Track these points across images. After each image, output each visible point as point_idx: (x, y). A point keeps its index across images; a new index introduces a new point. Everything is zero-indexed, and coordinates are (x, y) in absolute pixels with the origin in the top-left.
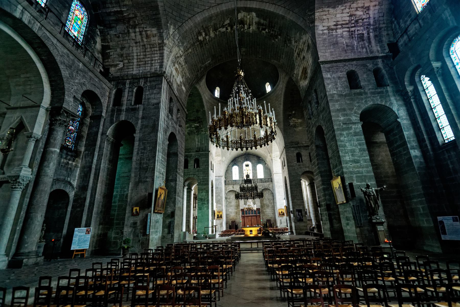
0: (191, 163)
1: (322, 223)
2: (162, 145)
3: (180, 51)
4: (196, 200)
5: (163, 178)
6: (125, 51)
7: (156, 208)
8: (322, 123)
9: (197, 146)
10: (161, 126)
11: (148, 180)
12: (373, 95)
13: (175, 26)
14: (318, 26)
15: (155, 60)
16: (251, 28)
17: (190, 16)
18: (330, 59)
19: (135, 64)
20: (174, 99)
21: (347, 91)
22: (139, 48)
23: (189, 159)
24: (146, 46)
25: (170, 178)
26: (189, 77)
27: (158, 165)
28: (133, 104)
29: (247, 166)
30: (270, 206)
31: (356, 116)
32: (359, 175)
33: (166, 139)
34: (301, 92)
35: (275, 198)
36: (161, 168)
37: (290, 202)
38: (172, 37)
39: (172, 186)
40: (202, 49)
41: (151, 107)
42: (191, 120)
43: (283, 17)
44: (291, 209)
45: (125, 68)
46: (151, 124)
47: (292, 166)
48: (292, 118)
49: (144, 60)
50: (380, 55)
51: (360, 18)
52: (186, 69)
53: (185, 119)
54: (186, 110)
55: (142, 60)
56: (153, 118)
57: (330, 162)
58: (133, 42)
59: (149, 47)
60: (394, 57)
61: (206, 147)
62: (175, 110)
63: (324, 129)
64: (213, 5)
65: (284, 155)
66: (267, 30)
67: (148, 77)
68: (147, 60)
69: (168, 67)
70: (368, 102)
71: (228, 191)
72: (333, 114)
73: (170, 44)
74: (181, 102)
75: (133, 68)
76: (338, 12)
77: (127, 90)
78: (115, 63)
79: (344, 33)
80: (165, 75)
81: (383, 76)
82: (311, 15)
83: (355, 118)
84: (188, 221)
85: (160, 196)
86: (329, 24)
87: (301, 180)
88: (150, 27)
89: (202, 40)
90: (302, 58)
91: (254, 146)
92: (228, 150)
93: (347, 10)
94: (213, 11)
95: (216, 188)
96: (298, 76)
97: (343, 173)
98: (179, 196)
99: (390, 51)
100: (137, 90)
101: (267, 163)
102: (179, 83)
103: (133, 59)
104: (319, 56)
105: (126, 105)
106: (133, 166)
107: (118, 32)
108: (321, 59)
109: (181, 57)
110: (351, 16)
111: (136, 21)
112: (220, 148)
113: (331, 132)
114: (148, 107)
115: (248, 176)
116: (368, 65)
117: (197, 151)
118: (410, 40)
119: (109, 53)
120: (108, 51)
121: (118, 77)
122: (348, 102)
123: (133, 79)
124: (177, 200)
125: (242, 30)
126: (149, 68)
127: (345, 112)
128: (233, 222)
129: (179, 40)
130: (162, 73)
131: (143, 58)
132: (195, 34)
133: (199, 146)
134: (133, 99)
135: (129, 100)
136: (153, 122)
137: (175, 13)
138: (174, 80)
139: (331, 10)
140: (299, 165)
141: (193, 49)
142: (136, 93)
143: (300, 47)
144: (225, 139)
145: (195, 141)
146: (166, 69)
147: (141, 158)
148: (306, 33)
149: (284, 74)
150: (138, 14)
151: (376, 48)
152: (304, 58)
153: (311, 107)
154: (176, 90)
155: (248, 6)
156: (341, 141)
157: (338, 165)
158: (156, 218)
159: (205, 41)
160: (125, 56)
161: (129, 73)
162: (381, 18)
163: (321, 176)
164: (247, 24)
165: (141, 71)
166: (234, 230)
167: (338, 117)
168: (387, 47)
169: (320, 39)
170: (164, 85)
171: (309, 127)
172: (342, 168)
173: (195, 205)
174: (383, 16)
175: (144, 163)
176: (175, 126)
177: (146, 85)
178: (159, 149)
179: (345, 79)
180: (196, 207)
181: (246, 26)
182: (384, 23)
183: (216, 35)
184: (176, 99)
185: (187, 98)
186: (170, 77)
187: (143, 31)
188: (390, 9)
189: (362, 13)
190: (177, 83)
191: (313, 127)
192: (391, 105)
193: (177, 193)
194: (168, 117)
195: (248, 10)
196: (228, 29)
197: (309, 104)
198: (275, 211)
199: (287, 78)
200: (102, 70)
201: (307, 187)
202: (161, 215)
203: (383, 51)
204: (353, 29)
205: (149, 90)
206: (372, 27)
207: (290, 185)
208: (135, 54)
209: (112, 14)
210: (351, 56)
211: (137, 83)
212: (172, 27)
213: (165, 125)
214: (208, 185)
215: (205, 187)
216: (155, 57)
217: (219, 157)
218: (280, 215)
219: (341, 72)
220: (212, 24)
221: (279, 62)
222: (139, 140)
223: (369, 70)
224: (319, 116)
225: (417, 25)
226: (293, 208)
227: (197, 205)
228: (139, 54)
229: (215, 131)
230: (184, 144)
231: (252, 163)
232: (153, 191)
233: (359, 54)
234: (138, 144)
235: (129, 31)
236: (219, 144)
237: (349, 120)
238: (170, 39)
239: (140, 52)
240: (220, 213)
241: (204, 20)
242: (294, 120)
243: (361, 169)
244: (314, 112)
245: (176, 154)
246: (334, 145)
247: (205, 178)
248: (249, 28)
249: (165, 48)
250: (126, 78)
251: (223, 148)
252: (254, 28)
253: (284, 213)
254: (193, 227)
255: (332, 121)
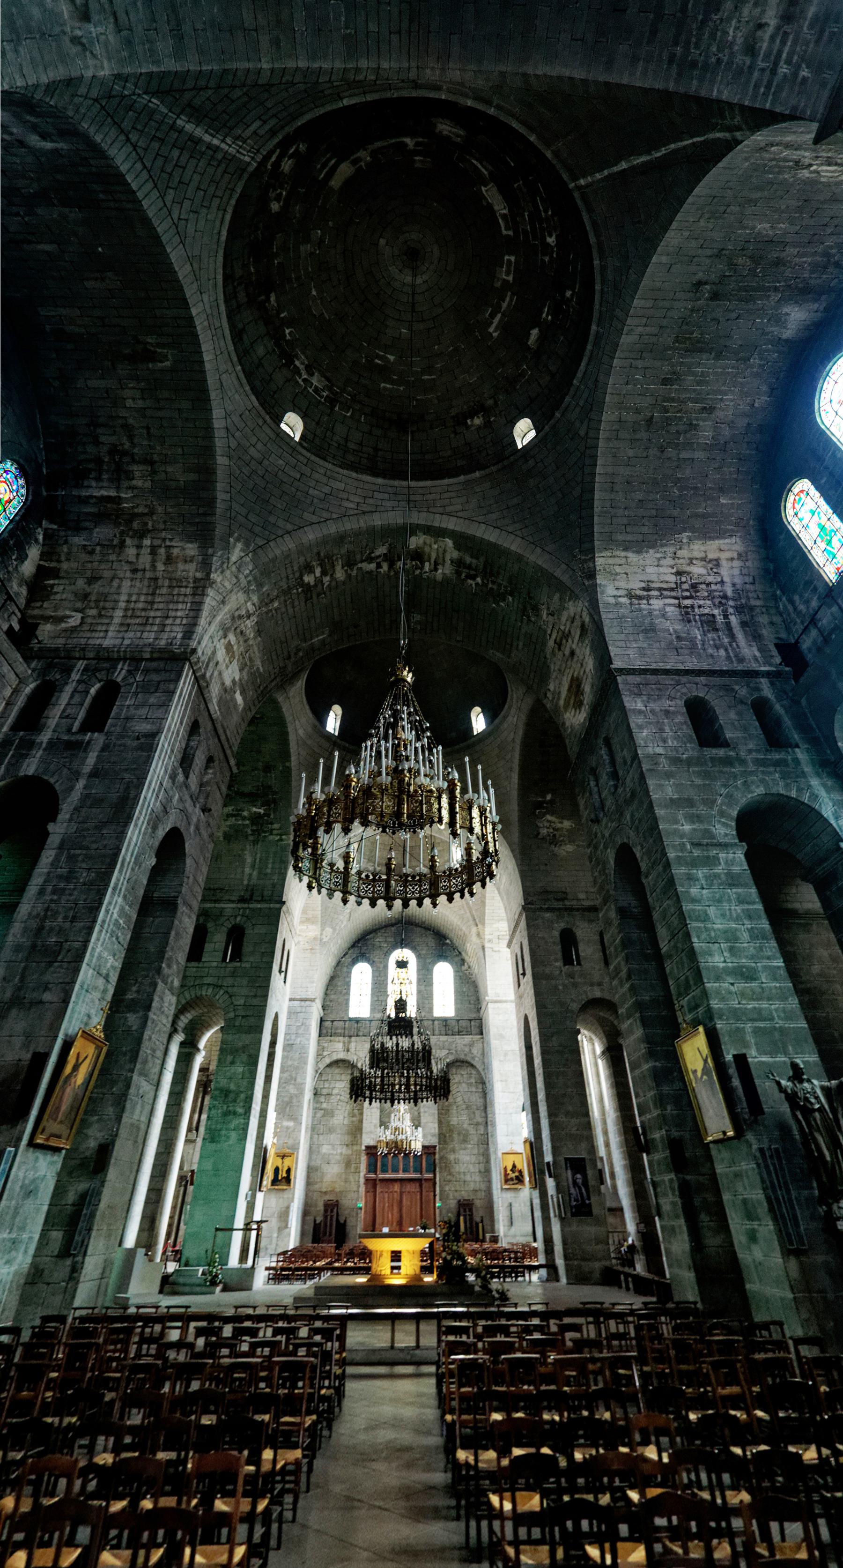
0: (217, 940)
1: (662, 1227)
2: (133, 869)
3: (249, 604)
4: (205, 1093)
5: (105, 991)
6: (96, 587)
7: (44, 1123)
8: (632, 837)
9: (245, 882)
10: (143, 805)
11: (47, 997)
12: (761, 769)
13: (247, 544)
14: (605, 586)
15: (176, 617)
16: (440, 571)
17: (289, 527)
18: (639, 664)
19: (116, 620)
20: (206, 726)
21: (691, 750)
22: (138, 584)
23: (210, 925)
24: (160, 582)
25: (129, 996)
26: (261, 670)
27: (98, 939)
28: (74, 729)
29: (402, 964)
30: (474, 1138)
31: (725, 825)
32: (761, 1024)
33: (151, 848)
34: (567, 741)
35: (492, 1105)
36: (105, 954)
37: (545, 1123)
38: (234, 568)
39: (129, 1031)
40: (309, 605)
41: (129, 742)
42: (242, 795)
43: (520, 558)
44: (548, 1158)
45: (86, 627)
46: (114, 796)
47: (548, 977)
48: (544, 814)
49: (143, 614)
50: (763, 669)
51: (702, 580)
52: (256, 649)
53: (224, 788)
54: (232, 762)
55: (138, 614)
56: (127, 776)
57: (668, 970)
58: (126, 567)
59: (167, 583)
60: (797, 676)
61: (274, 885)
62: (199, 760)
63: (638, 855)
64: (352, 512)
65: (522, 935)
66: (479, 580)
67: (142, 659)
68: (152, 614)
69: (206, 638)
70: (753, 787)
71: (328, 1061)
72: (659, 812)
73: (227, 584)
74: (223, 738)
75: (106, 631)
76: (648, 562)
77: (69, 689)
78: (60, 613)
79: (668, 609)
80: (194, 659)
81: (778, 722)
82: (585, 561)
83: (724, 830)
84: (153, 1197)
85: (76, 1068)
86: (630, 586)
87: (578, 1032)
88: (181, 540)
89: (312, 583)
90: (567, 652)
91: (430, 896)
92: (345, 901)
93: (669, 561)
94: (349, 525)
95: (288, 1047)
96: (559, 698)
97: (710, 1014)
98: (144, 1074)
99: (786, 661)
100: (98, 692)
101: (466, 958)
102: (228, 683)
103: (113, 609)
104: (612, 655)
105: (54, 731)
106: (10, 938)
107: (95, 540)
108: (617, 664)
109: (249, 617)
110: (679, 573)
111: (150, 524)
112: (319, 892)
113: (660, 868)
114: (119, 742)
115: (401, 1005)
116: (737, 687)
117: (242, 900)
118: (826, 640)
119: (52, 586)
120: (51, 582)
121: (57, 649)
122: (698, 781)
123: (98, 658)
124: (132, 1091)
125: (418, 572)
126: (153, 635)
127: (694, 811)
128: (332, 1207)
129: (250, 578)
130: (185, 652)
131: (144, 610)
132: (295, 568)
133: (254, 881)
134: (82, 715)
135: (67, 717)
136: (121, 790)
137: (253, 518)
138: (216, 673)
139: (633, 557)
140: (571, 976)
141: (285, 601)
142: (95, 699)
143: (562, 628)
144: (340, 865)
145: (243, 862)
146: (199, 643)
147: (47, 910)
148: (574, 597)
149: (522, 690)
150: (160, 510)
151: (749, 651)
152: (572, 653)
153: (597, 785)
154: (215, 701)
155: (437, 524)
156: (694, 901)
157: (692, 982)
158: (31, 1175)
159: (320, 586)
160: (93, 598)
161: (91, 642)
162: (751, 587)
163: (644, 1022)
164: (429, 561)
165: (127, 642)
166: (330, 1247)
167: (676, 822)
168: (775, 652)
169: (611, 616)
170: (185, 686)
171: (596, 848)
172: (705, 994)
173: (196, 1116)
174: (753, 583)
175: (51, 929)
176: (190, 809)
177: (132, 680)
178: (118, 880)
179: (682, 718)
180: (197, 1129)
181: (427, 564)
182: (758, 598)
183: (349, 577)
184: (209, 726)
185: (244, 726)
186: (207, 665)
187: (160, 546)
188: (767, 571)
189: (703, 571)
190: (223, 684)
191: (606, 848)
192: (815, 800)
193: (140, 1059)
194: (173, 777)
195: (439, 533)
196: (381, 567)
197: (592, 778)
198: (488, 1161)
199: (529, 701)
200: (17, 627)
201: (600, 1062)
202: (55, 1158)
203: (767, 658)
204: (688, 602)
205: (136, 694)
206: (731, 603)
207: (544, 1053)
208: (124, 598)
209: (92, 501)
210: (691, 663)
211: (108, 670)
212: (239, 546)
213: (158, 803)
214: (261, 1032)
215: (246, 1039)
216: (177, 610)
217: (312, 927)
218: (507, 1180)
219: (671, 698)
220: (343, 551)
221: (509, 657)
222: (61, 847)
223: (742, 702)
224: (621, 815)
225: (835, 609)
226: (555, 1150)
227: (204, 1117)
228: (134, 598)
229: (313, 835)
230: (205, 870)
231: (419, 956)
232: (51, 1048)
233: (710, 661)
234: (51, 859)
235: (124, 541)
236: (318, 881)
237: (708, 833)
238: (228, 573)
239: (139, 594)
240: (287, 1162)
241: (325, 541)
242: (550, 822)
243: (764, 1005)
244: (609, 802)
245: (170, 906)
246: (672, 910)
247: (255, 1002)
248: (436, 569)
249: (211, 592)
250: (77, 655)
251: (330, 895)
252: (447, 572)
253: (520, 1172)
254: (170, 1226)
255: (659, 833)
